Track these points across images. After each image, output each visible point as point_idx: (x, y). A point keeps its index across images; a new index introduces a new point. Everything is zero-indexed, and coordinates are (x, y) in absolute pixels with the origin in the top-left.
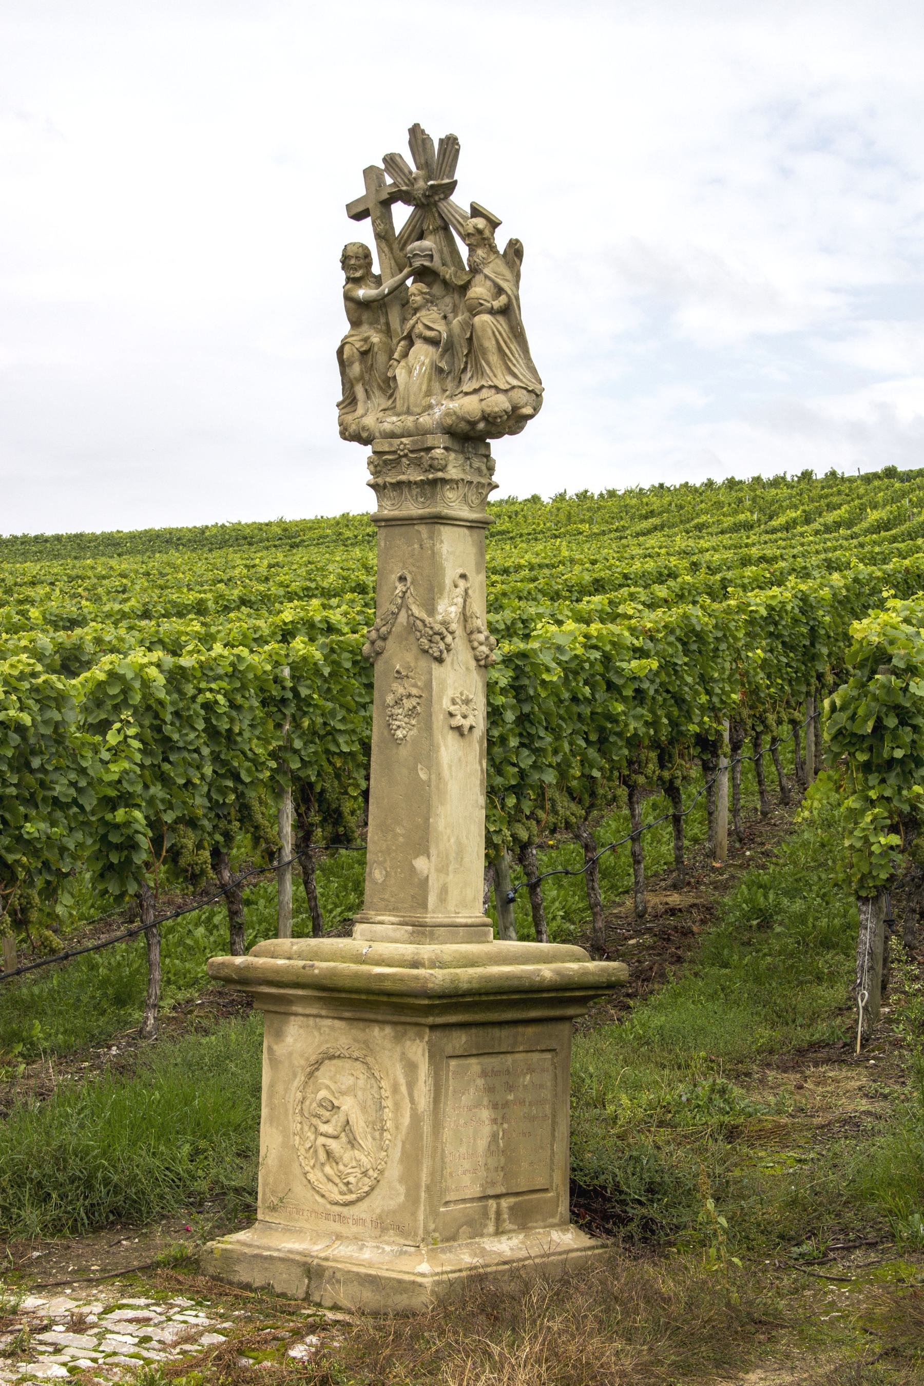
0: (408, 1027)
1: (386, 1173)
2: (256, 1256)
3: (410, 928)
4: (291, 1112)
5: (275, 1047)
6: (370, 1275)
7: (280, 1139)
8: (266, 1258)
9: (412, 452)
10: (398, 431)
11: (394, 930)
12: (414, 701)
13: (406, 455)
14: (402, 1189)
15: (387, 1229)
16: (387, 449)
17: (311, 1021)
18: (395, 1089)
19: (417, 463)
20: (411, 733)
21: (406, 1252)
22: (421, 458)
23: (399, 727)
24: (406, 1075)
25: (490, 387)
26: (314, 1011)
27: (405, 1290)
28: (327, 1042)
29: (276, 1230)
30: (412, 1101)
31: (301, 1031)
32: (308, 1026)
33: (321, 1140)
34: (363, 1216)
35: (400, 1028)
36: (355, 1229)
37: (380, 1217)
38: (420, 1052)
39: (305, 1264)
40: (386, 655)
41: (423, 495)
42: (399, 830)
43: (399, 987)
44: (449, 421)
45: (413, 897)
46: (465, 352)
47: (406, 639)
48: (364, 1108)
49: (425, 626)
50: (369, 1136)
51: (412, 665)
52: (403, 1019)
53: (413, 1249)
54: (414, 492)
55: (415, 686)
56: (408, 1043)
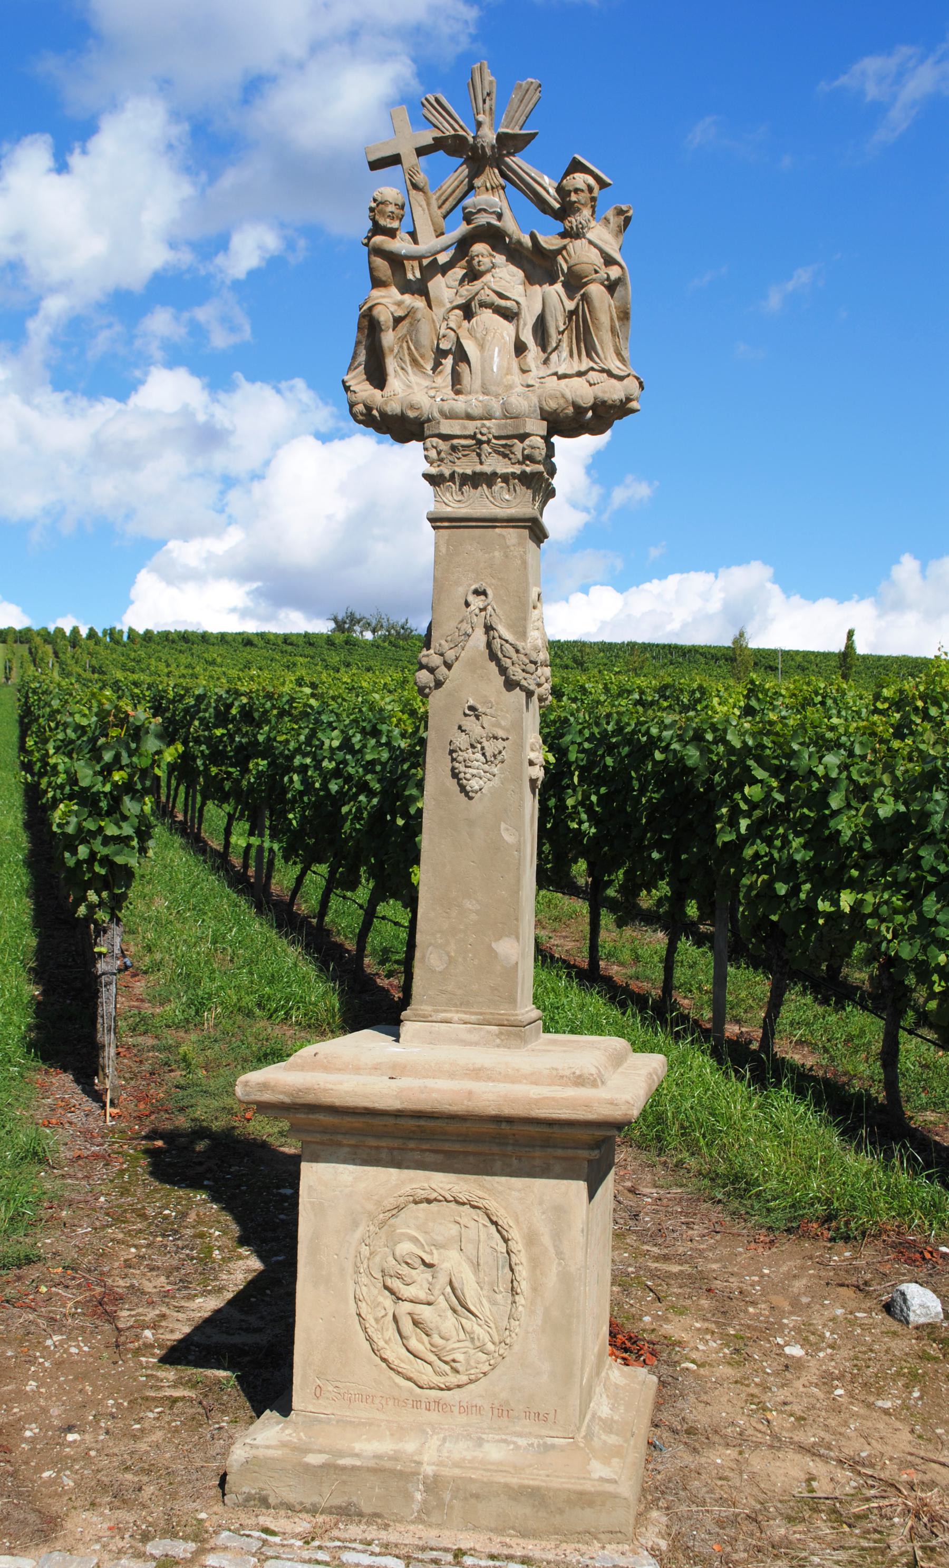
8: (344, 1469)
9: (496, 438)
11: (470, 1031)
12: (500, 745)
13: (488, 442)
16: (458, 433)
20: (490, 784)
21: (553, 1446)
33: (406, 1307)
34: (479, 1402)
42: (468, 904)
49: (517, 651)
50: (484, 1301)
55: (498, 725)
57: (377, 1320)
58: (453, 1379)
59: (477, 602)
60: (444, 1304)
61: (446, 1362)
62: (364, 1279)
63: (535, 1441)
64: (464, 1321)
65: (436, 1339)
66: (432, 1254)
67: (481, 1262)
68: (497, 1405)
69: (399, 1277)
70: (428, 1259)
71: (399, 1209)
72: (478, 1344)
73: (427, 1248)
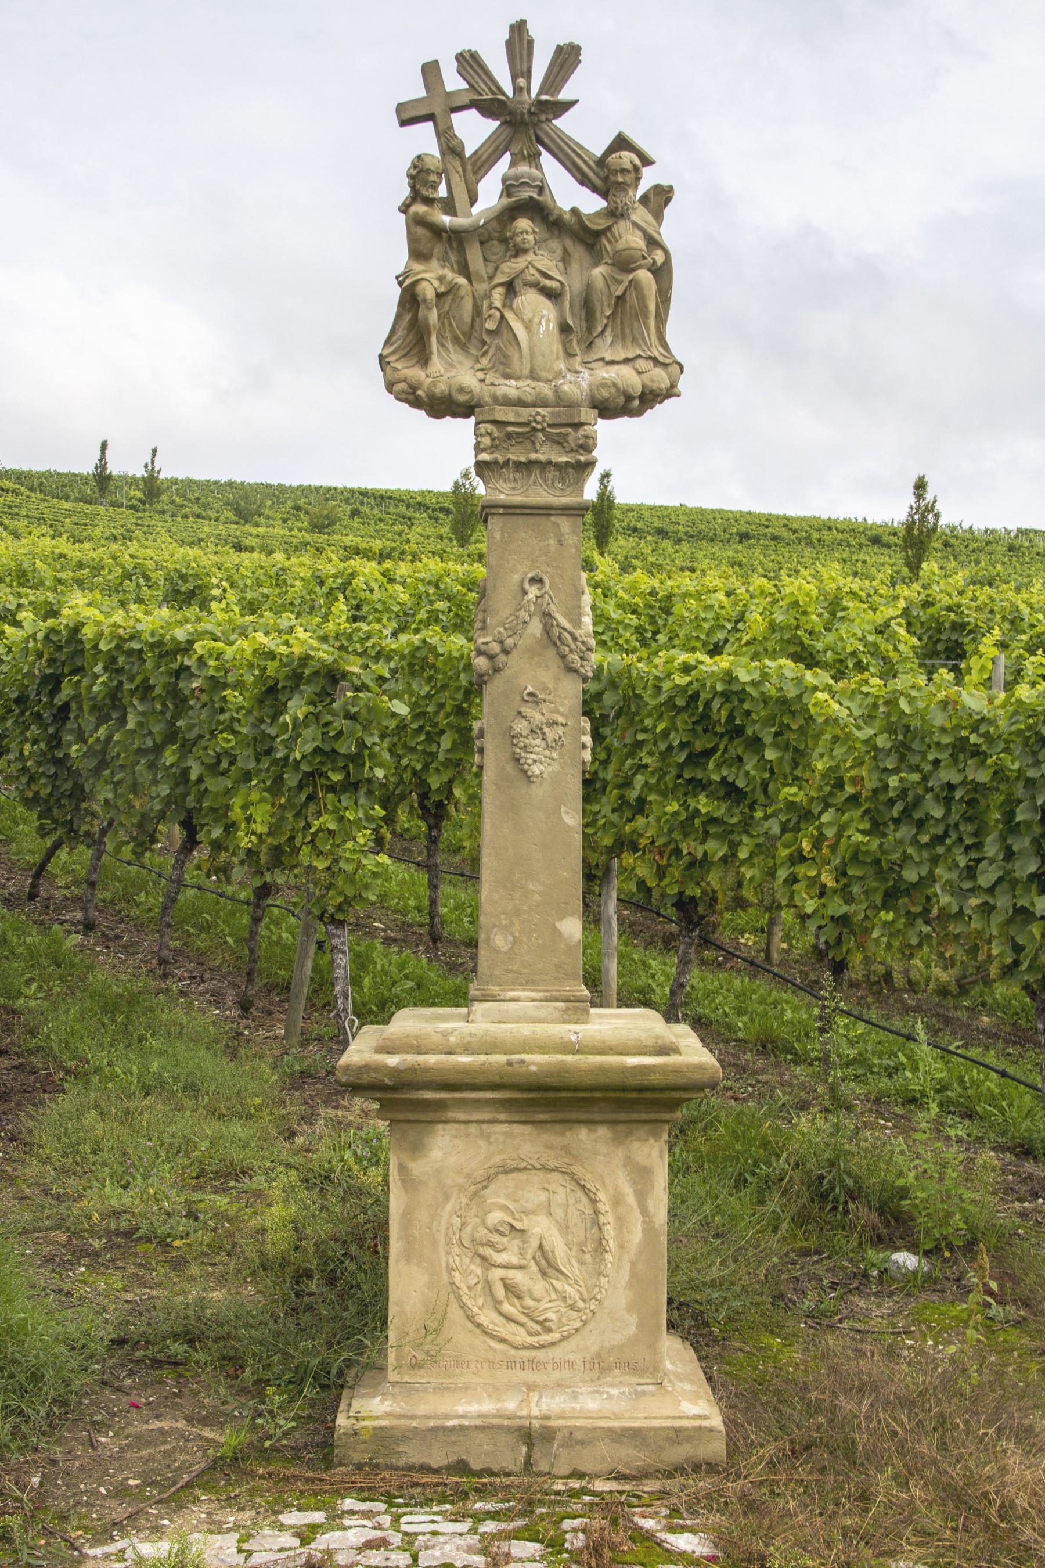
0: (634, 1126)
1: (606, 1303)
2: (434, 1430)
3: (562, 1004)
4: (442, 1242)
5: (411, 1165)
6: (631, 1429)
7: (425, 1278)
8: (453, 1429)
9: (549, 425)
10: (529, 399)
11: (537, 1008)
12: (560, 730)
13: (543, 430)
14: (633, 1319)
15: (610, 1369)
16: (512, 420)
17: (473, 1129)
18: (617, 1200)
19: (559, 442)
20: (551, 769)
21: (644, 1393)
22: (567, 435)
23: (535, 761)
24: (633, 1183)
25: (650, 358)
26: (487, 1116)
27: (689, 1439)
28: (500, 1152)
29: (426, 1391)
30: (644, 1212)
31: (457, 1142)
32: (467, 1135)
33: (497, 1274)
34: (571, 1357)
35: (621, 1128)
36: (556, 1375)
37: (598, 1355)
38: (655, 1153)
39: (520, 1429)
40: (507, 672)
41: (562, 479)
42: (531, 886)
43: (671, 1080)
44: (605, 394)
45: (558, 967)
46: (608, 313)
47: (540, 654)
48: (564, 1228)
49: (575, 639)
50: (574, 1262)
51: (551, 686)
52: (634, 1116)
53: (652, 1388)
54: (550, 476)
55: (557, 712)
56: (636, 1144)
57: (469, 1288)
58: (545, 1338)
59: (533, 591)
60: (534, 1268)
61: (538, 1322)
62: (457, 1250)
63: (626, 1389)
64: (554, 1282)
65: (529, 1302)
66: (521, 1220)
67: (570, 1224)
68: (588, 1357)
69: (491, 1245)
70: (518, 1225)
71: (489, 1179)
72: (569, 1302)
73: (517, 1216)
